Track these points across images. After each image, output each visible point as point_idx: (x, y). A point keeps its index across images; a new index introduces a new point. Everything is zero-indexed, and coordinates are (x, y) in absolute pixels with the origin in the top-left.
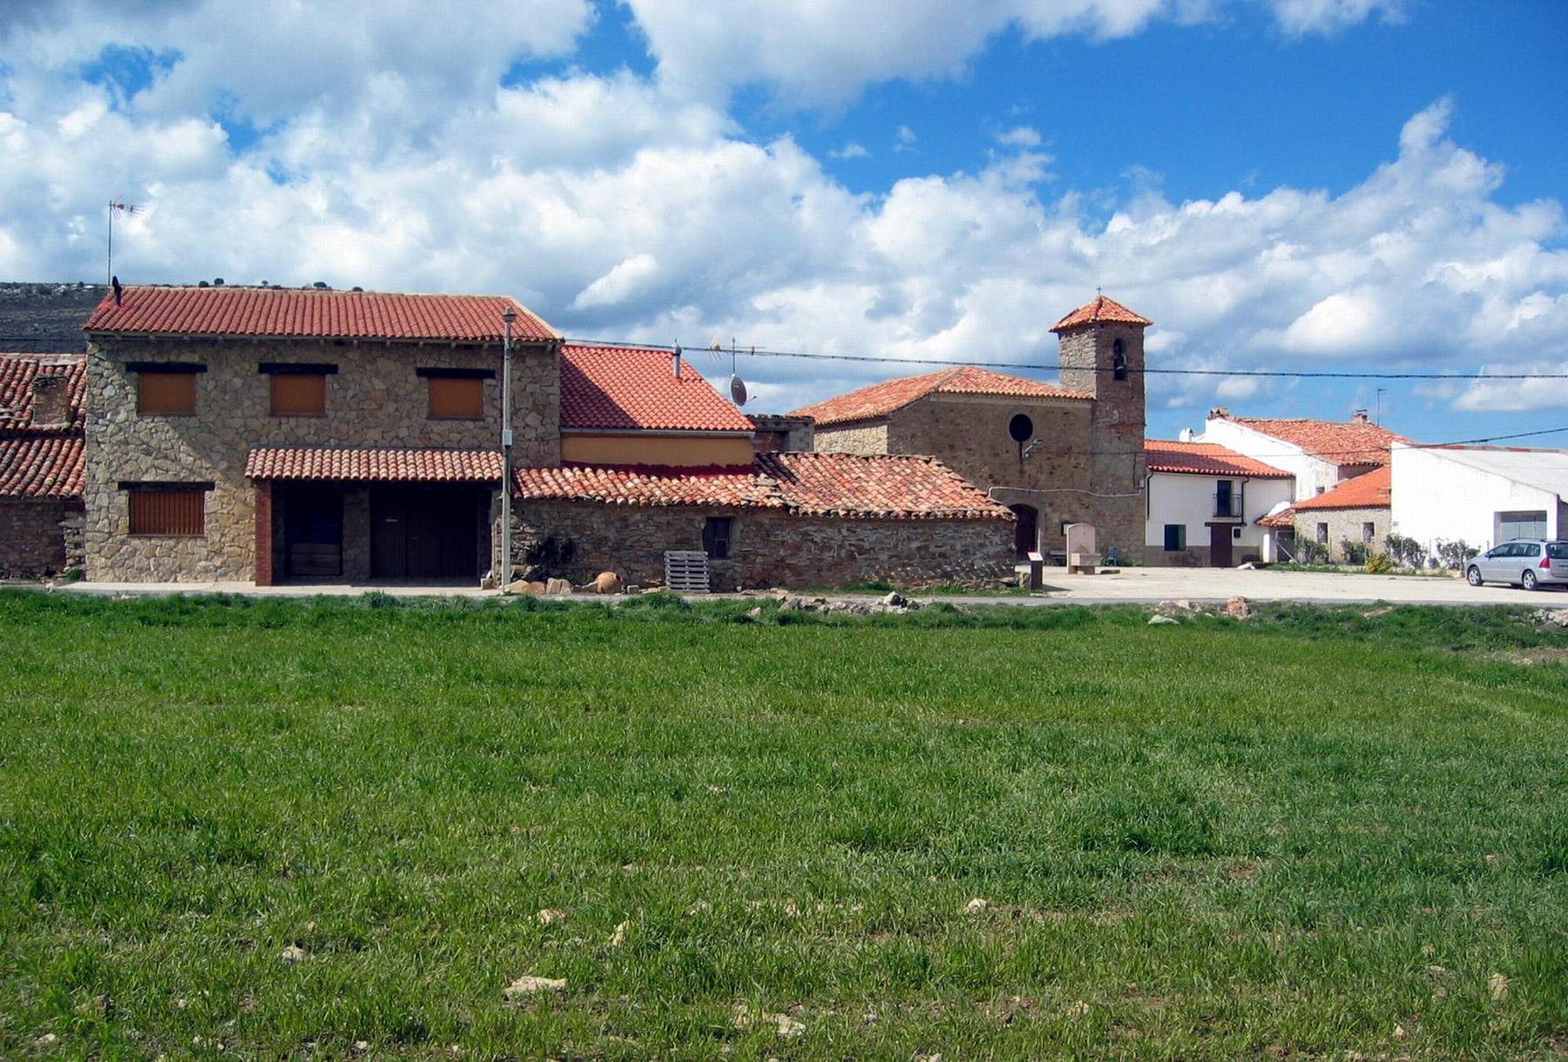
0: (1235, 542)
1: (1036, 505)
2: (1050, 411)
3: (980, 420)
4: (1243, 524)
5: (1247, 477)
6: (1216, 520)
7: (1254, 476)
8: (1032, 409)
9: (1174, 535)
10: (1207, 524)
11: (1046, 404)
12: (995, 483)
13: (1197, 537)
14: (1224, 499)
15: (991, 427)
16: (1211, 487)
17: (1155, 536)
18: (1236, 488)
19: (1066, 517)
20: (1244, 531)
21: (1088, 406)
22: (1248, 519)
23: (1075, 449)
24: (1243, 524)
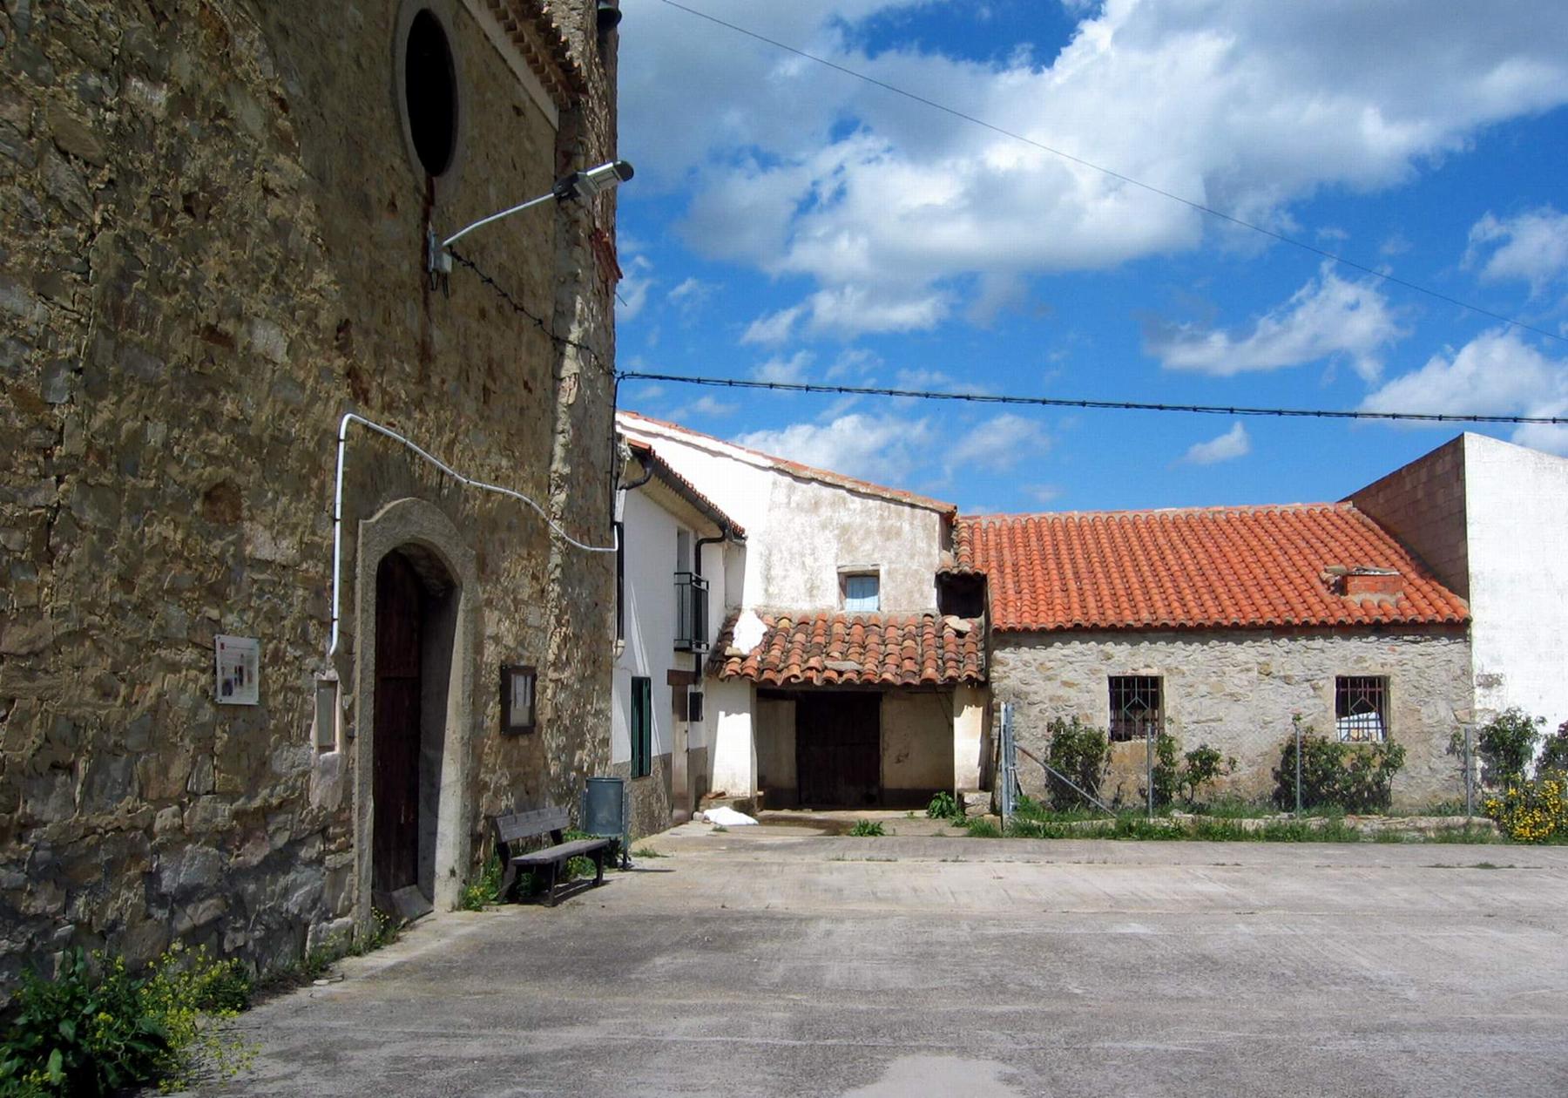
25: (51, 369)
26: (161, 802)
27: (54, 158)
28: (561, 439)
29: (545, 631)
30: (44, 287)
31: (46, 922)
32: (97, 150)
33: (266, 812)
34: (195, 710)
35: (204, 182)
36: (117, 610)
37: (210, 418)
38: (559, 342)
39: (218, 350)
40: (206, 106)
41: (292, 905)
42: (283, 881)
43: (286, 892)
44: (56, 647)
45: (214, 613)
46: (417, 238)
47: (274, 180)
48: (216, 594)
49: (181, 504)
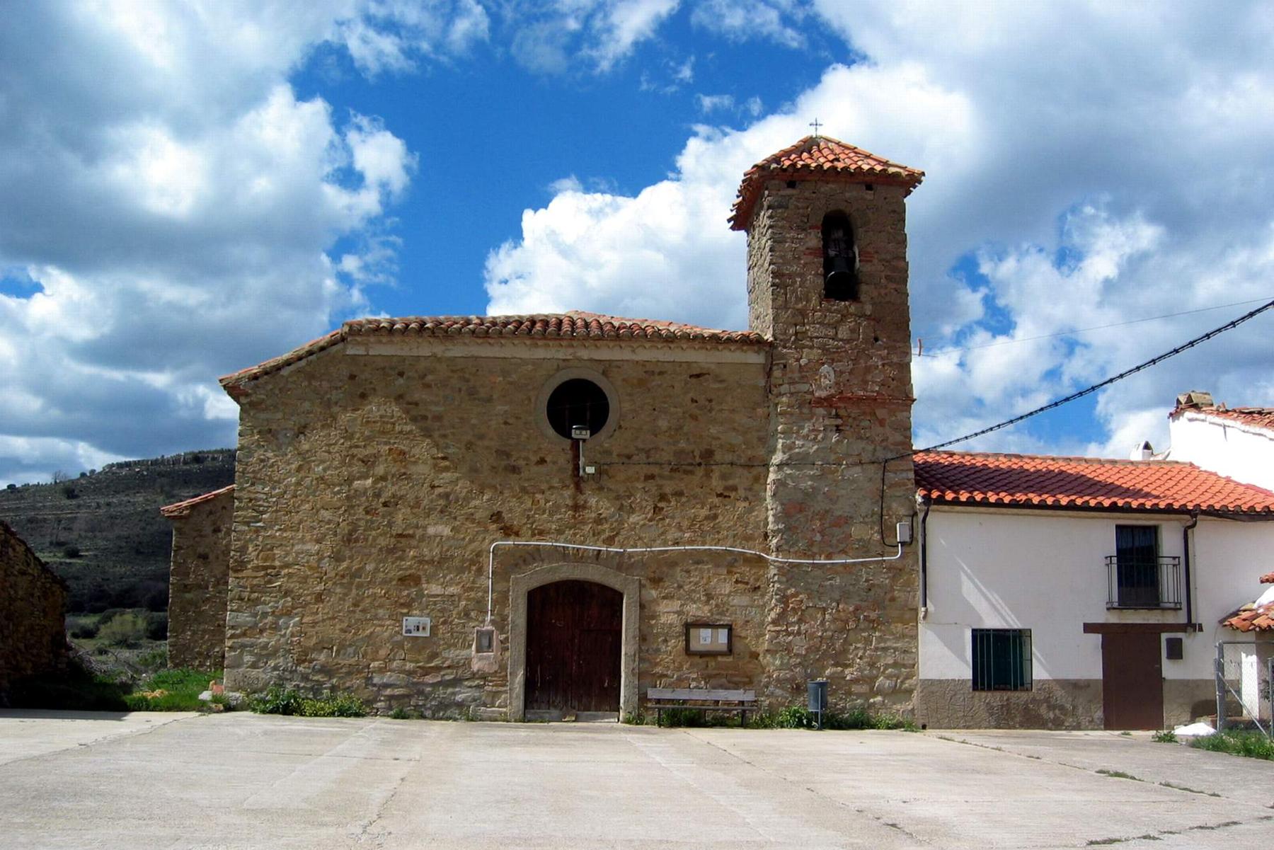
0: (1170, 670)
1: (613, 580)
2: (651, 372)
3: (472, 393)
4: (1192, 626)
5: (1191, 516)
6: (1113, 618)
7: (1212, 512)
8: (607, 368)
9: (999, 657)
10: (1089, 628)
11: (647, 354)
12: (508, 531)
13: (1064, 655)
14: (1137, 564)
15: (500, 408)
16: (1100, 539)
17: (944, 658)
18: (1170, 543)
19: (696, 610)
20: (1190, 643)
21: (755, 358)
22: (1206, 613)
23: (718, 457)
24: (1192, 626)
25: (320, 560)
26: (374, 660)
27: (322, 511)
28: (771, 513)
29: (764, 606)
30: (318, 541)
31: (321, 684)
32: (339, 504)
33: (438, 669)
34: (391, 636)
35: (394, 496)
36: (354, 612)
37: (401, 558)
38: (766, 466)
39: (403, 540)
40: (393, 476)
41: (459, 698)
42: (450, 690)
43: (454, 694)
44: (324, 620)
45: (405, 611)
46: (570, 467)
47: (436, 483)
48: (408, 605)
49: (384, 582)
